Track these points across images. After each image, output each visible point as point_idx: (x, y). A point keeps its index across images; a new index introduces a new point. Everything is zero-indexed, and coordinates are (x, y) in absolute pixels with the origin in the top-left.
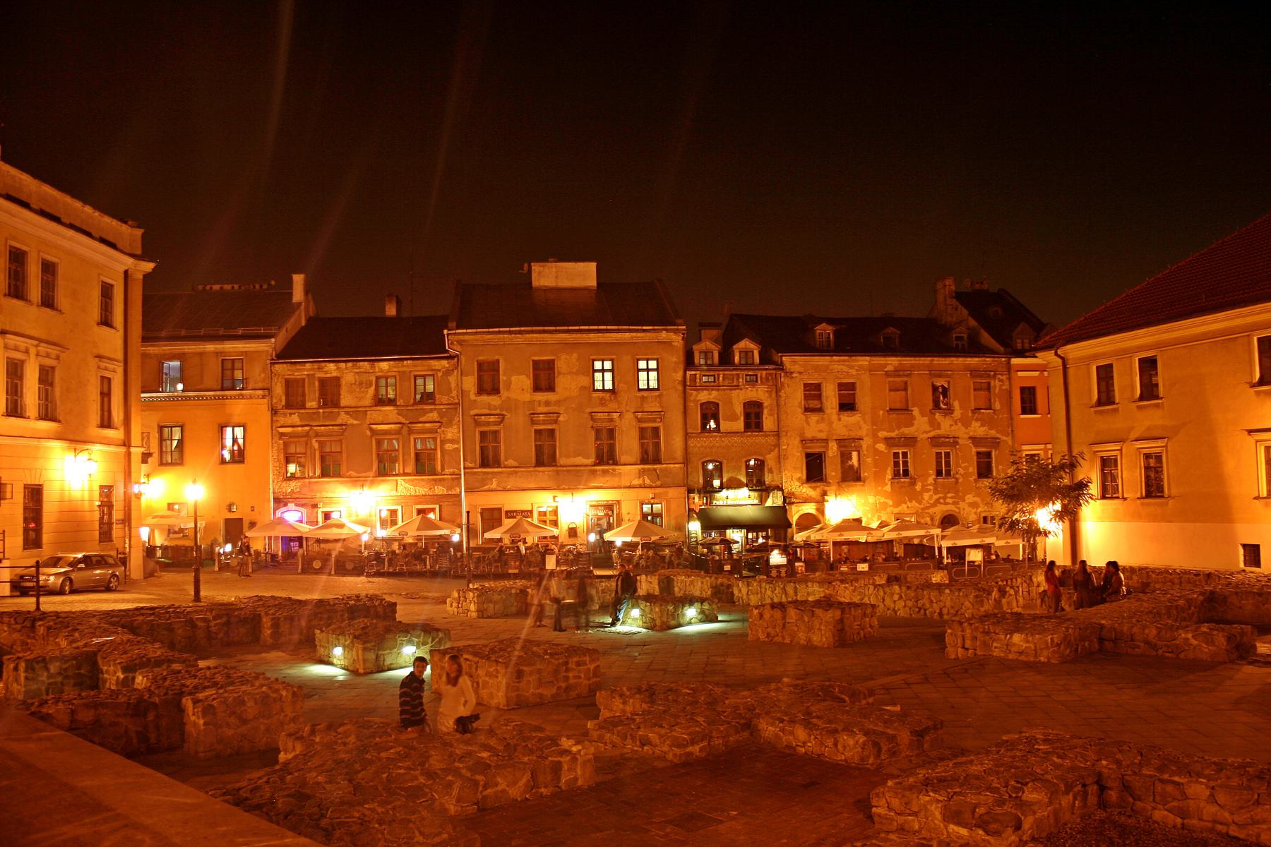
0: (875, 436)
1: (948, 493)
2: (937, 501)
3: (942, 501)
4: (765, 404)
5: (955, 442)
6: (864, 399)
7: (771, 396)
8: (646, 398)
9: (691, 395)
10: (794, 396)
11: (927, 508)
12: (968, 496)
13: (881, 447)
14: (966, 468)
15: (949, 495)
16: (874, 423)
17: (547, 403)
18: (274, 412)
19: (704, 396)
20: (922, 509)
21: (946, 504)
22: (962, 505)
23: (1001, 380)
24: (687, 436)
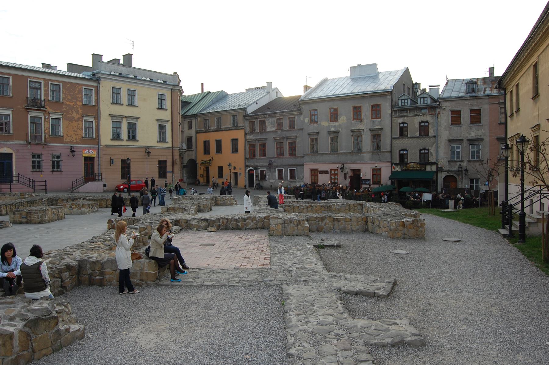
6: (485, 118)
7: (433, 119)
8: (375, 122)
9: (395, 120)
17: (335, 127)
18: (246, 134)
19: (401, 120)
24: (392, 139)
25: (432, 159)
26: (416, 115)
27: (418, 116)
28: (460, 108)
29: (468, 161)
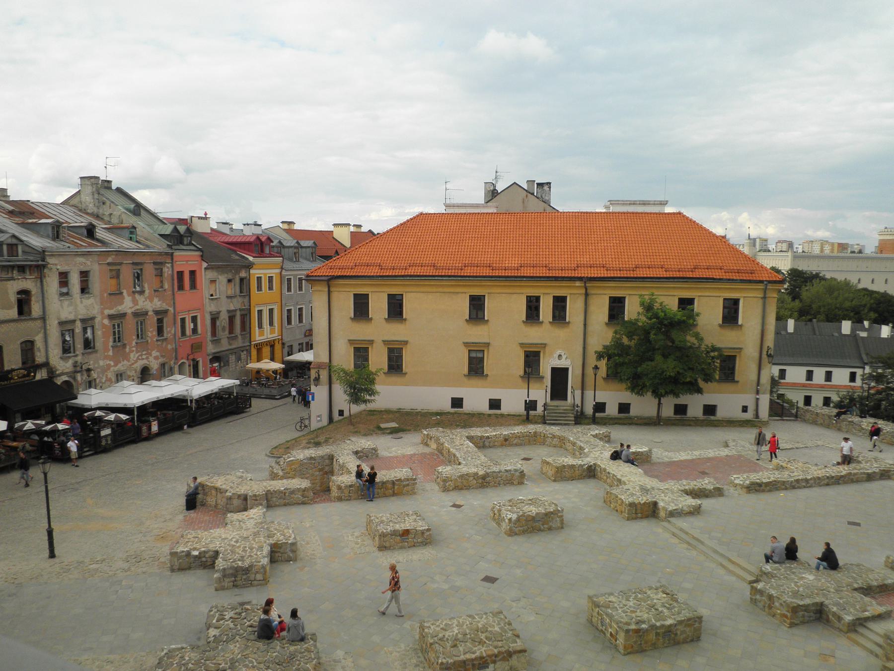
0: (102, 313)
1: (143, 351)
2: (138, 358)
3: (140, 358)
4: (33, 293)
5: (146, 313)
7: (36, 286)
10: (52, 283)
11: (133, 364)
12: (154, 352)
13: (106, 322)
14: (152, 332)
15: (144, 353)
16: (102, 304)
20: (130, 365)
21: (143, 359)
22: (151, 359)
23: (168, 268)
25: (40, 358)
26: (13, 279)
27: (14, 280)
28: (69, 268)
29: (83, 354)
